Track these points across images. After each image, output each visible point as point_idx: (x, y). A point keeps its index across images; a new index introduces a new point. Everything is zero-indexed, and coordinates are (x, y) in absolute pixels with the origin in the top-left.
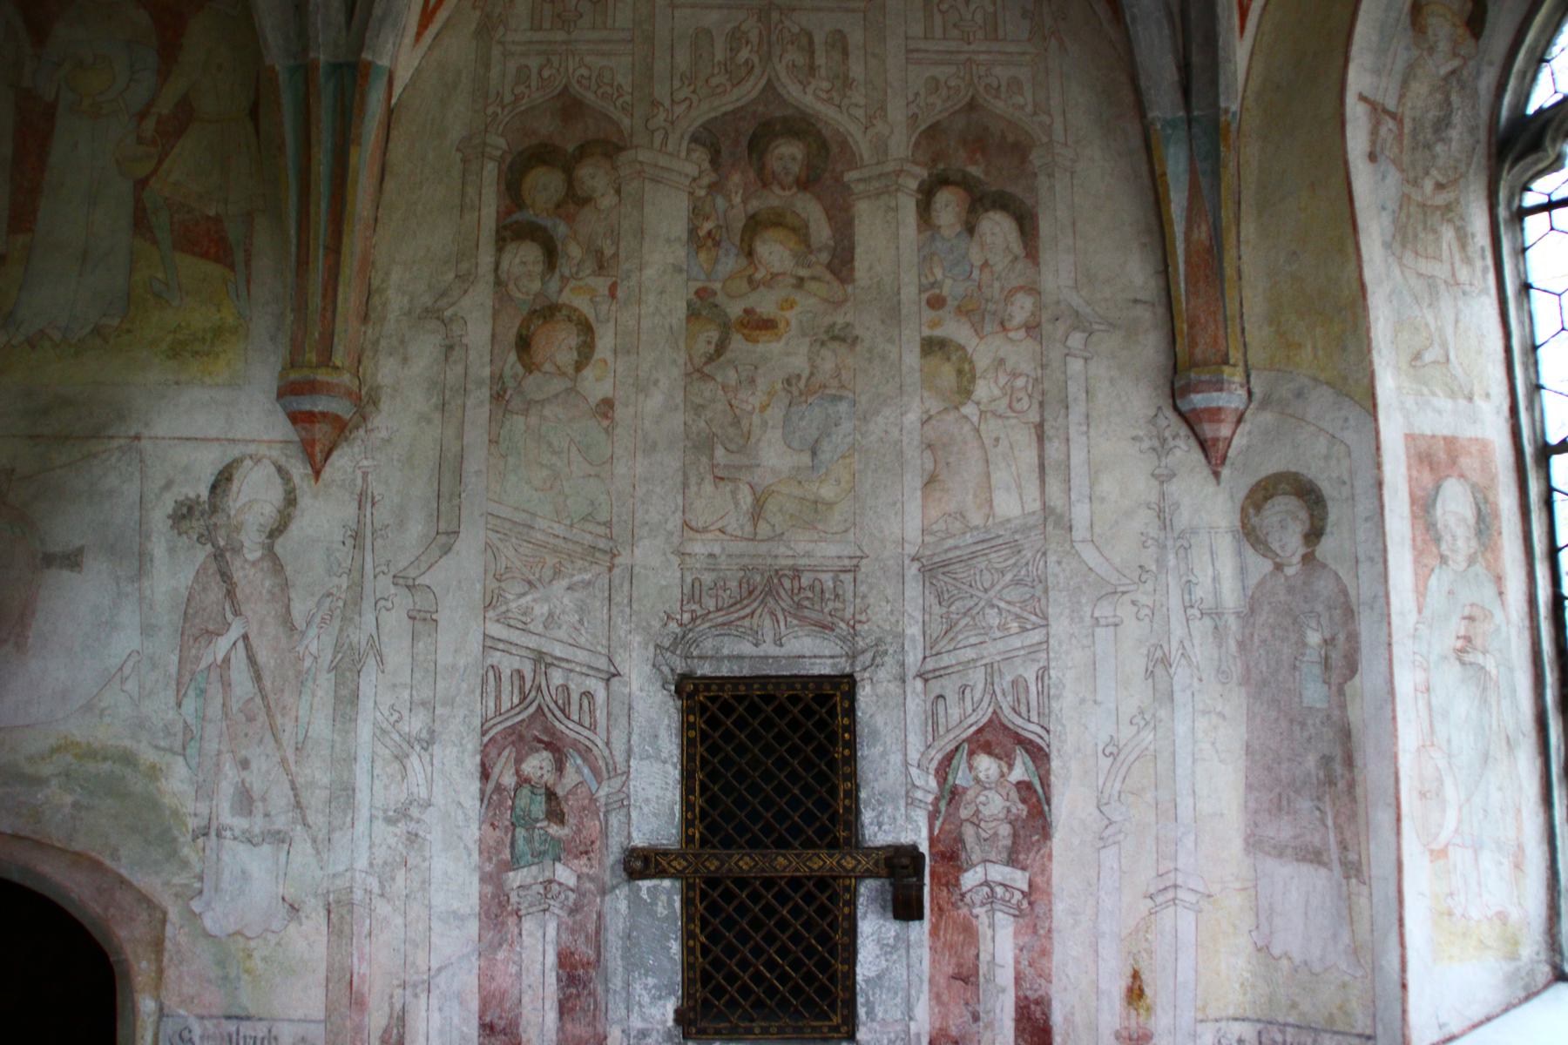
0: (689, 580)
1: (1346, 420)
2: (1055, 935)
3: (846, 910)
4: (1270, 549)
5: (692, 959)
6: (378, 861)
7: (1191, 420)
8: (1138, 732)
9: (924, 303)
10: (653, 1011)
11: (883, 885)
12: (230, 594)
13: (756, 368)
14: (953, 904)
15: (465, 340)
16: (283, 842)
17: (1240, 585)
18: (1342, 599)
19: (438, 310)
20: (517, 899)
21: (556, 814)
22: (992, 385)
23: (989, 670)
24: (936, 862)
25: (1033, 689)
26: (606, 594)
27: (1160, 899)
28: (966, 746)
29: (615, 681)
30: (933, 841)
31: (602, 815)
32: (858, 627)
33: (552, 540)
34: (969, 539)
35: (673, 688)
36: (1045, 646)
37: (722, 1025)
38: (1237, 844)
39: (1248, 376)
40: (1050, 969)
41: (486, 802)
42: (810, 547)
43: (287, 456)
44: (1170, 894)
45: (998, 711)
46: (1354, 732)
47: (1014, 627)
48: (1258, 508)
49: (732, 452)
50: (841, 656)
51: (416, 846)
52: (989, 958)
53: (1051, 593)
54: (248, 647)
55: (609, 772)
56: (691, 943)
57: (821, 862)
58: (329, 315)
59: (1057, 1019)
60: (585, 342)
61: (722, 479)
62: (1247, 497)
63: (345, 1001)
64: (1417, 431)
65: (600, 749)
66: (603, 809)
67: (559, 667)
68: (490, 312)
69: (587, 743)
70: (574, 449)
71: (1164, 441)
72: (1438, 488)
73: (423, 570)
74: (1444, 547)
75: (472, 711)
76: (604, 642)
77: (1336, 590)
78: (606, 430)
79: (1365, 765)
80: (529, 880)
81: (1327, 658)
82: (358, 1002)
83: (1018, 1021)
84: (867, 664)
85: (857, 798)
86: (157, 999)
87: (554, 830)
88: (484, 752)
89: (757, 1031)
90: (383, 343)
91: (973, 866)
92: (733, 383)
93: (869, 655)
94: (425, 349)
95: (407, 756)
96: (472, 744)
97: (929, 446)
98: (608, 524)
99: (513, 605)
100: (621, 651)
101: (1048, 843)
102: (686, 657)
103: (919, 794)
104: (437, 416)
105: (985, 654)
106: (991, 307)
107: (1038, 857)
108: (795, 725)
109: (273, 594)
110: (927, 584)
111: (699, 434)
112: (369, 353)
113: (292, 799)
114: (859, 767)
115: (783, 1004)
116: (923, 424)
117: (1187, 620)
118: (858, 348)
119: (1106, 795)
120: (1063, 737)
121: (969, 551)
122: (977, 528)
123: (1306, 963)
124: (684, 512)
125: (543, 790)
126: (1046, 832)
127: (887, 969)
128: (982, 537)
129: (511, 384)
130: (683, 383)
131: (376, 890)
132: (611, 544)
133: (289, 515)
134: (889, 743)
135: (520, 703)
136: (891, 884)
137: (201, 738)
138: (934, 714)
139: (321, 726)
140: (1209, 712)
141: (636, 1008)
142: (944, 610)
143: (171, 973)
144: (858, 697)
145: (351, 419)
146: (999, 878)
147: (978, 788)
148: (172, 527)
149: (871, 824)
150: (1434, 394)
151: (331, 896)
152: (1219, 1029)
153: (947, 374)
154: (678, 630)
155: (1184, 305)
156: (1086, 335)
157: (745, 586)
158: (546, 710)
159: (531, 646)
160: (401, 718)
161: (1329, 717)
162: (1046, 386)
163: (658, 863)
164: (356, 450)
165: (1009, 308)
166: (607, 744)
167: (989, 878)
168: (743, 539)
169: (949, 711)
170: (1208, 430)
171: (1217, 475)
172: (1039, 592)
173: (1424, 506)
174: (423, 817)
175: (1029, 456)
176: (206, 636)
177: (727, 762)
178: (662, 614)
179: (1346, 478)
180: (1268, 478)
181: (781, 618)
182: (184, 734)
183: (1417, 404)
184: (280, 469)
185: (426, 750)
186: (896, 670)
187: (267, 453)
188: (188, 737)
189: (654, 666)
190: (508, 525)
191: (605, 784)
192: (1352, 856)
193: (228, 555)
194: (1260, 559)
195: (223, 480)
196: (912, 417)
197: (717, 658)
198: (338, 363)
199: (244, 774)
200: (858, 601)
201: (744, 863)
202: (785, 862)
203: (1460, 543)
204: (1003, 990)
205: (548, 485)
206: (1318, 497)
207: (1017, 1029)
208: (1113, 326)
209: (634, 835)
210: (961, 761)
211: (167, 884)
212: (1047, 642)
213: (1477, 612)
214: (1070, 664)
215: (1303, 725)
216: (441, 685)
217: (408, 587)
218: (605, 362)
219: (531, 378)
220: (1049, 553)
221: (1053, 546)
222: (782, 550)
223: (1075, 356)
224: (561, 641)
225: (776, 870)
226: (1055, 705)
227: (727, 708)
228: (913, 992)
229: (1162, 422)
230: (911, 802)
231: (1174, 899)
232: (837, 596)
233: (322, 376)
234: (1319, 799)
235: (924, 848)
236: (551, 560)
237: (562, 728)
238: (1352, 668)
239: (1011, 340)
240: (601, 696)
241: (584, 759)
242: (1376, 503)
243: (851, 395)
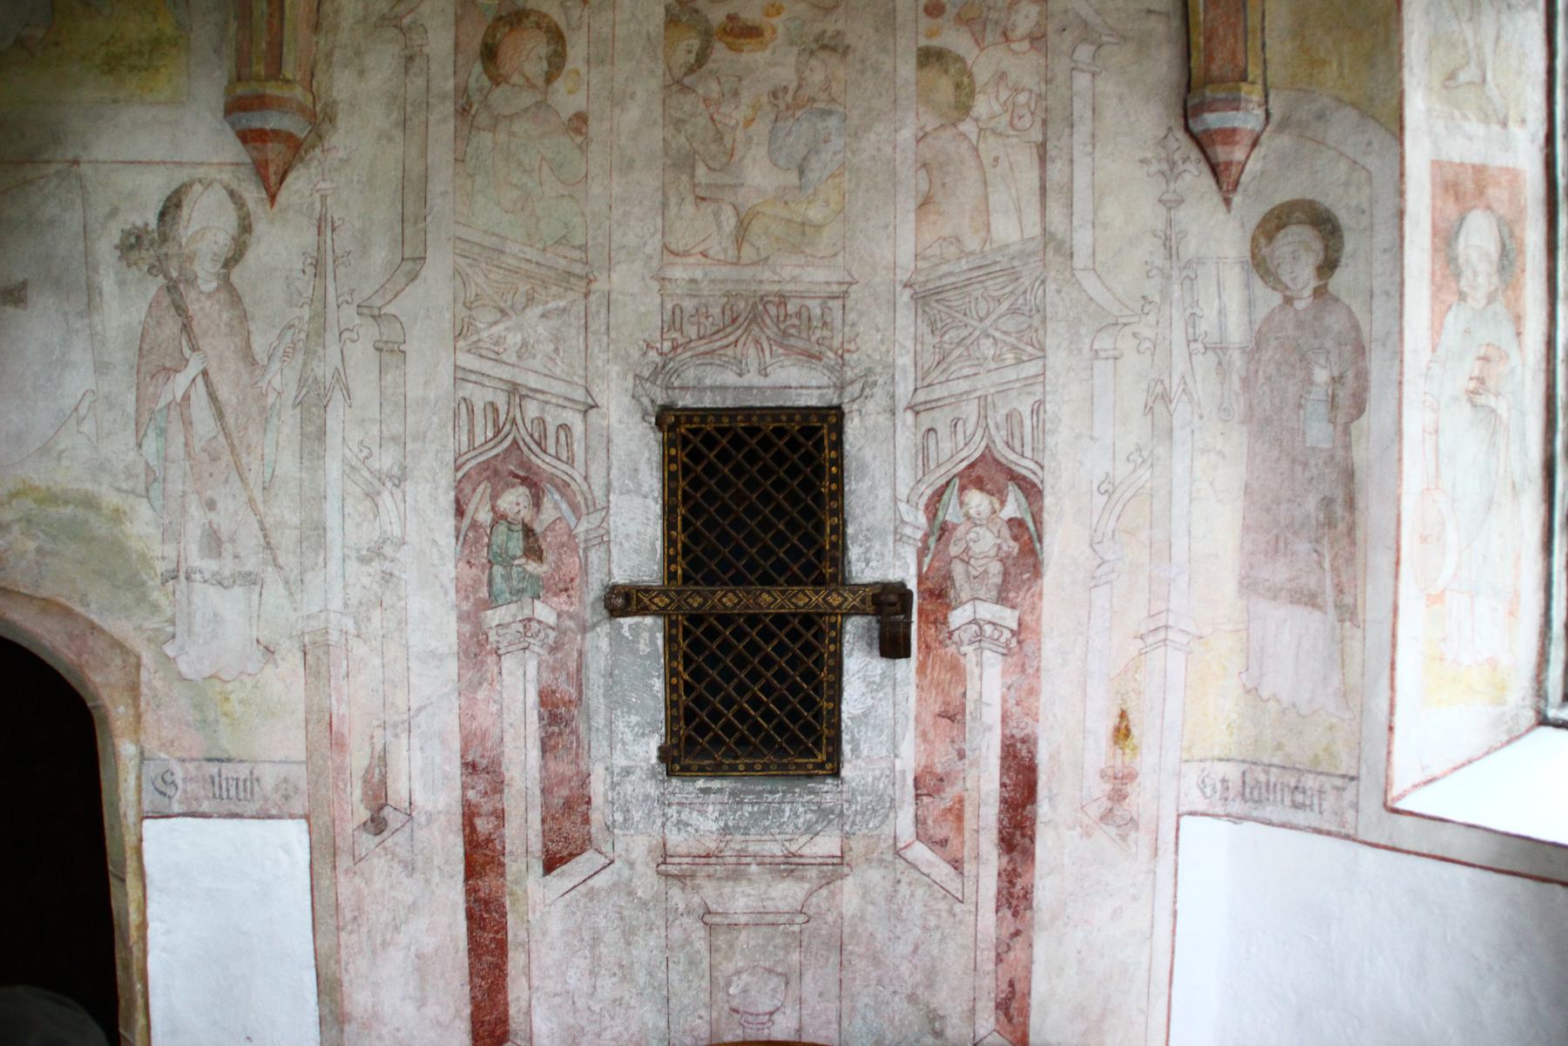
0: (669, 306)
1: (1369, 144)
2: (1043, 675)
3: (832, 648)
4: (1278, 280)
5: (675, 697)
6: (354, 602)
7: (1202, 142)
8: (1135, 470)
9: (921, 9)
10: (636, 748)
11: (870, 623)
12: (186, 327)
13: (740, 79)
14: (940, 642)
15: (426, 50)
16: (254, 584)
17: (1246, 318)
18: (1353, 335)
19: (396, 17)
20: (496, 638)
21: (534, 551)
22: (994, 102)
23: (982, 403)
25: (1027, 422)
26: (583, 322)
27: (1150, 640)
28: (957, 481)
29: (592, 412)
30: (921, 579)
31: (581, 551)
32: (847, 356)
33: (524, 266)
34: (964, 265)
35: (653, 420)
36: (1041, 379)
37: (706, 762)
38: (1230, 586)
39: (1267, 96)
40: (1037, 708)
41: (461, 538)
42: (797, 271)
43: (239, 180)
44: (1161, 635)
45: (992, 445)
46: (1358, 474)
47: (1010, 357)
48: (1270, 238)
49: (715, 170)
50: (829, 387)
51: (391, 586)
52: (976, 696)
53: (1049, 324)
54: (208, 384)
55: (587, 507)
56: (674, 680)
57: (806, 599)
58: (276, 21)
59: (1043, 759)
60: (555, 51)
61: (703, 199)
62: (1259, 226)
63: (326, 742)
64: (1444, 158)
65: (578, 485)
66: (582, 546)
67: (534, 399)
68: (451, 19)
69: (565, 478)
70: (545, 169)
71: (1173, 165)
72: (1462, 219)
73: (388, 299)
74: (1463, 283)
75: (444, 446)
76: (581, 372)
77: (1348, 325)
78: (580, 147)
79: (1367, 508)
80: (508, 619)
81: (1333, 397)
82: (338, 743)
83: (1004, 759)
84: (856, 395)
85: (844, 533)
86: (137, 742)
87: (532, 567)
88: (458, 487)
89: (741, 767)
90: (337, 55)
91: (962, 604)
92: (715, 95)
93: (857, 387)
94: (383, 63)
95: (379, 493)
96: (446, 479)
97: (924, 165)
98: (584, 248)
99: (485, 334)
100: (598, 381)
101: (1039, 582)
102: (667, 388)
103: (908, 531)
104: (398, 134)
105: (979, 386)
106: (993, 15)
108: (780, 458)
109: (232, 327)
110: (920, 311)
111: (679, 150)
112: (321, 66)
113: (261, 537)
114: (846, 502)
115: (768, 741)
116: (918, 141)
117: (1190, 355)
118: (850, 57)
119: (1100, 533)
121: (963, 278)
122: (972, 253)
123: (1294, 705)
124: (663, 234)
125: (520, 527)
126: (1037, 570)
127: (873, 707)
128: (978, 263)
129: (476, 98)
130: (661, 96)
131: (352, 630)
132: (587, 268)
133: (245, 243)
134: (877, 476)
135: (495, 437)
136: (878, 621)
137: (164, 479)
138: (925, 448)
139: (288, 465)
140: (1209, 451)
141: (619, 746)
142: (937, 340)
143: (149, 718)
144: (846, 429)
145: (306, 137)
146: (988, 617)
147: (969, 525)
148: (120, 258)
149: (858, 560)
150: (1465, 117)
151: (307, 639)
152: (1203, 770)
153: (944, 88)
154: (658, 359)
155: (1202, 17)
156: (1093, 48)
157: (728, 312)
158: (521, 443)
159: (504, 377)
160: (371, 454)
161: (1332, 457)
162: (1051, 101)
163: (639, 601)
164: (313, 171)
165: (1013, 17)
166: (586, 478)
168: (726, 263)
169: (941, 445)
170: (1221, 153)
171: (1227, 202)
172: (1036, 322)
173: (1446, 239)
174: (398, 555)
175: (1030, 178)
176: (163, 373)
177: (710, 496)
178: (641, 343)
179: (1365, 206)
180: (1282, 205)
181: (766, 345)
182: (147, 475)
183: (1446, 128)
184: (232, 194)
185: (398, 486)
186: (885, 402)
187: (218, 177)
188: (151, 478)
189: (633, 397)
190: (477, 250)
191: (584, 519)
192: (1348, 600)
193: (182, 286)
194: (1269, 292)
195: (171, 207)
196: (906, 134)
197: (700, 389)
198: (289, 76)
199: (212, 515)
201: (728, 600)
202: (770, 599)
203: (1481, 279)
204: (990, 728)
205: (519, 206)
206: (1334, 227)
207: (1002, 767)
208: (1124, 39)
209: (615, 571)
210: (951, 497)
211: (139, 628)
212: (1044, 374)
213: (1492, 353)
214: (1067, 398)
215: (1305, 465)
216: (411, 419)
217: (373, 317)
218: (577, 72)
219: (498, 91)
220: (1048, 282)
221: (1053, 274)
222: (767, 275)
223: (1083, 71)
224: (536, 372)
225: (761, 607)
226: (1050, 441)
227: (709, 441)
228: (899, 730)
229: (1173, 145)
230: (900, 538)
231: (1165, 640)
232: (825, 324)
233: (271, 89)
234: (1317, 541)
235: (912, 585)
236: (524, 287)
237: (539, 462)
238: (1359, 406)
239: (1014, 52)
240: (578, 428)
241: (563, 495)
242: (1396, 234)
243: (841, 109)
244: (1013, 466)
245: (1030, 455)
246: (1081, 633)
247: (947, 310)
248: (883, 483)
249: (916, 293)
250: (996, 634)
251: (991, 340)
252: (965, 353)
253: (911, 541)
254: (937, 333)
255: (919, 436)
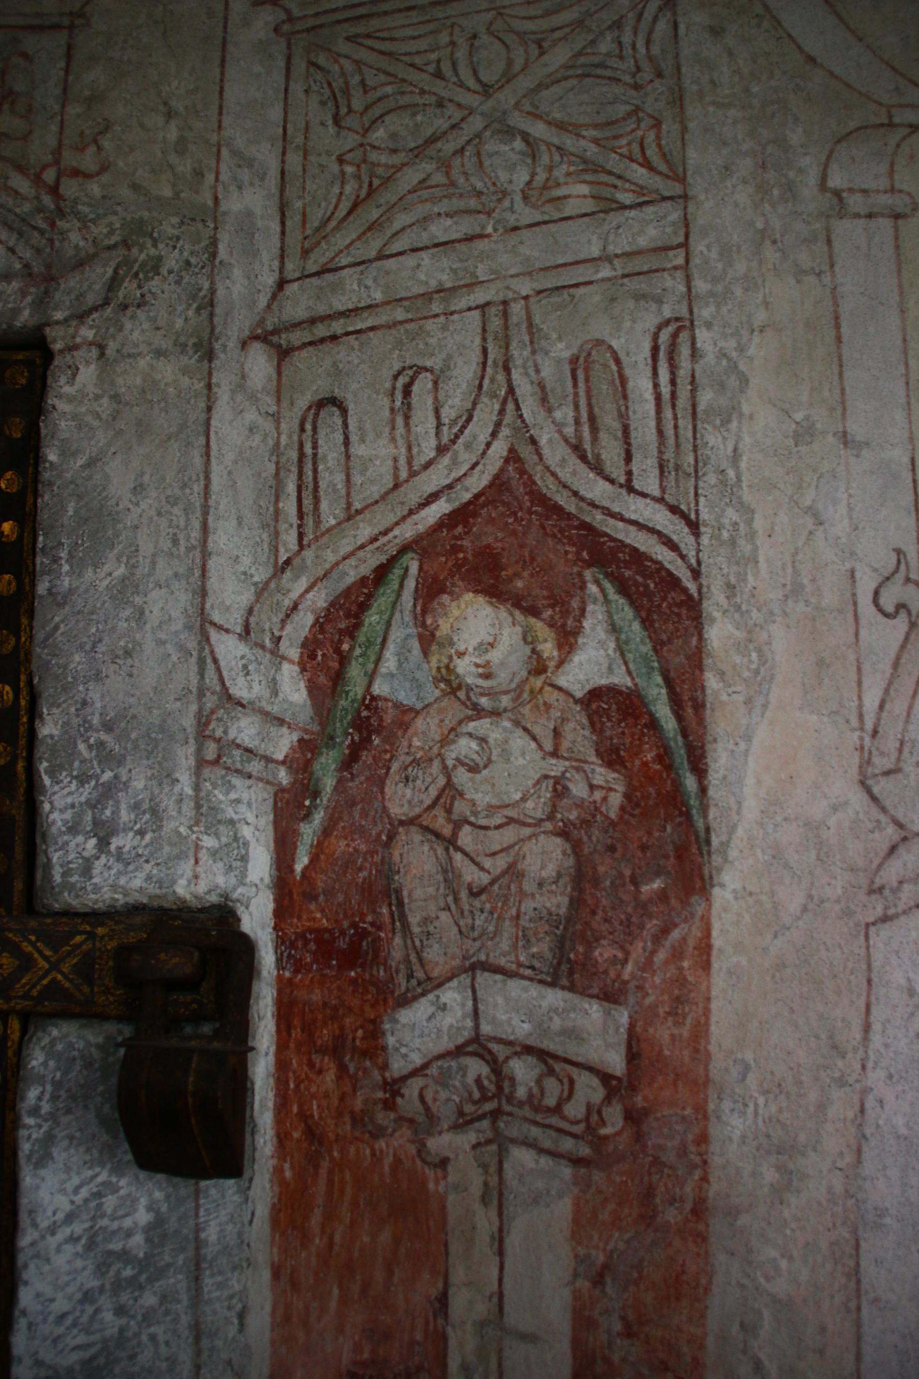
2: (717, 1226)
14: (357, 1120)
23: (495, 323)
24: (298, 967)
32: (70, 188)
45: (526, 452)
52: (482, 1308)
53: (693, 110)
84: (91, 299)
93: (100, 274)
107: (661, 956)
110: (299, 65)
120: (745, 547)
134: (146, 548)
142: (352, 140)
146: (522, 1029)
147: (454, 711)
149: (73, 829)
167: (486, 1029)
169: (359, 450)
200: (73, 110)
212: (685, 245)
214: (761, 316)
244: (597, 519)
245: (653, 488)
246: (841, 1082)
247: (383, 62)
248: (164, 570)
249: (290, 19)
250: (553, 1091)
251: (518, 144)
252: (439, 178)
253: (255, 767)
254: (348, 122)
255: (290, 425)
